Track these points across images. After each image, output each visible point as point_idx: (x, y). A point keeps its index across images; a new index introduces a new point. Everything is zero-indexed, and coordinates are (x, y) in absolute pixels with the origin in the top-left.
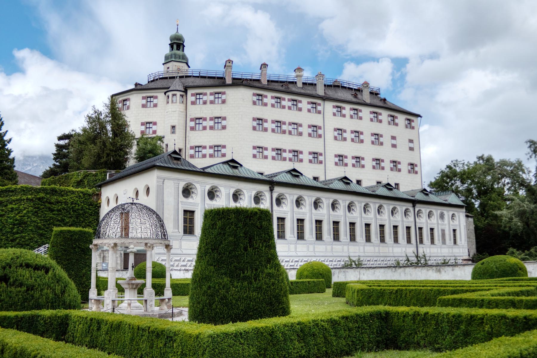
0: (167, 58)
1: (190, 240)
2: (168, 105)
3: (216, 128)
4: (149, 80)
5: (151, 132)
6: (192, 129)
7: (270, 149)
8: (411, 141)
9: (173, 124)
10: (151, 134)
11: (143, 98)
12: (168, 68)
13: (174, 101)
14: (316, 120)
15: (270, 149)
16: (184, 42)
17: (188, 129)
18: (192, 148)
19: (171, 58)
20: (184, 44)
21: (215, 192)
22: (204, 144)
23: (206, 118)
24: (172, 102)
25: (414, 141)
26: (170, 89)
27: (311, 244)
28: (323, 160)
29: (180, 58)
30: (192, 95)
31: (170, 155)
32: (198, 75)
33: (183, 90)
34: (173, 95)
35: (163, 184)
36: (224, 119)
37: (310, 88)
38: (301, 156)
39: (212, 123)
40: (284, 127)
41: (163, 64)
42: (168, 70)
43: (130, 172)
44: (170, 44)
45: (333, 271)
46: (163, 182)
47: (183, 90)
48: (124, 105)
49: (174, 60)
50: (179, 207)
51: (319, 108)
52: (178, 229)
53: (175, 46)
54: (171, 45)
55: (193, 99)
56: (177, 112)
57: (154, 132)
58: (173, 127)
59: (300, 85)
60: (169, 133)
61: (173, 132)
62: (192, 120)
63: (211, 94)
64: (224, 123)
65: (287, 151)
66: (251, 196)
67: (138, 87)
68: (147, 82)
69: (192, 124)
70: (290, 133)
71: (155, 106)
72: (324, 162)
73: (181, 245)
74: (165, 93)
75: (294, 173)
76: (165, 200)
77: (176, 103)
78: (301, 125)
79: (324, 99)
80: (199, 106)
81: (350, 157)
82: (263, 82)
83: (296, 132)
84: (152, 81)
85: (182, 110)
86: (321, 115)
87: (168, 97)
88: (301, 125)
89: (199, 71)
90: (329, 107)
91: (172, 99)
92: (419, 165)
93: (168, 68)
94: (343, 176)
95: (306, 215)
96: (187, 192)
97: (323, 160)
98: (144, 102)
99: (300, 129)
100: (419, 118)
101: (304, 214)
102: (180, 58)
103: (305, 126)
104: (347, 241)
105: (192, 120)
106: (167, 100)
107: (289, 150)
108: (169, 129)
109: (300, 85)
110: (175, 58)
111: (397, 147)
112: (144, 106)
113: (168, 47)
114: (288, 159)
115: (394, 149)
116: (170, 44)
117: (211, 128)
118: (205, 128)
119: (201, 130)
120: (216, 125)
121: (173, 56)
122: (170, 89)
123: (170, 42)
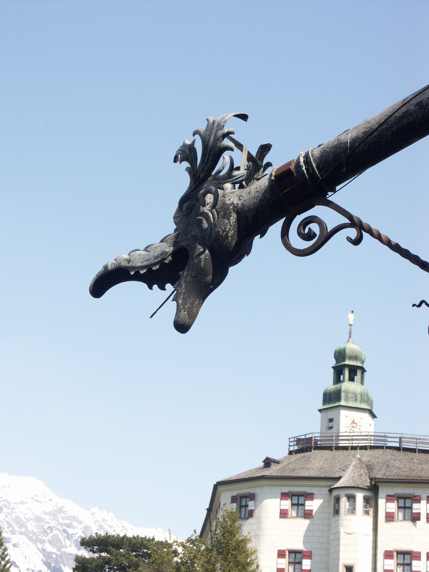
4: (292, 449)
11: (284, 496)
16: (363, 362)
20: (365, 366)
23: (419, 553)
29: (356, 400)
30: (390, 498)
32: (397, 445)
41: (320, 411)
42: (330, 425)
44: (333, 367)
48: (241, 506)
55: (392, 507)
62: (388, 555)
67: (272, 471)
68: (287, 452)
74: (331, 491)
84: (297, 452)
87: (337, 500)
89: (401, 435)
102: (356, 400)
105: (388, 555)
106: (335, 505)
110: (346, 400)
113: (331, 373)
116: (333, 367)
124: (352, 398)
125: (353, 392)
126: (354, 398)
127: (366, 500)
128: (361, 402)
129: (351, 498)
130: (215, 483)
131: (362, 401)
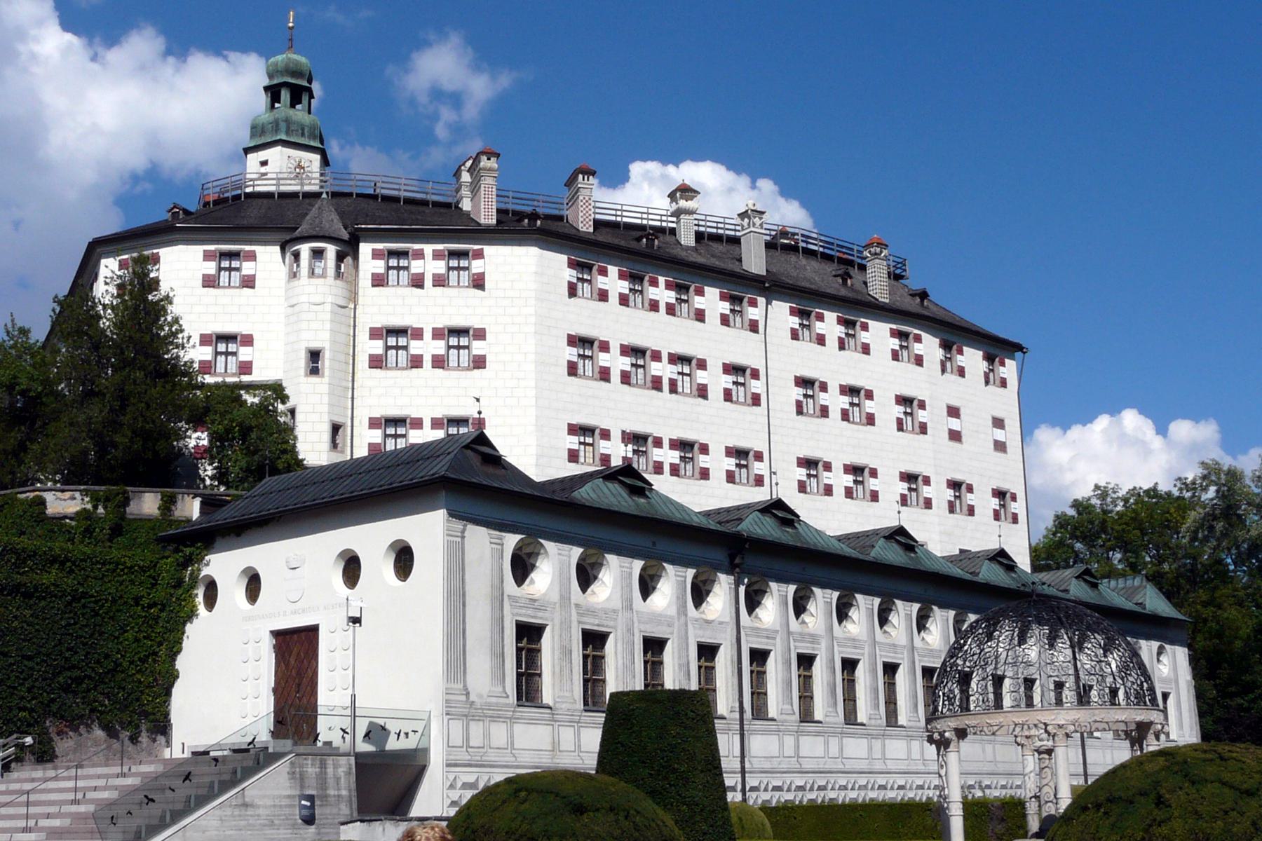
0: (257, 130)
1: (532, 722)
2: (295, 283)
3: (453, 361)
5: (232, 367)
6: (377, 362)
7: (616, 435)
8: (998, 423)
9: (315, 345)
10: (233, 375)
11: (208, 256)
12: (264, 163)
13: (318, 271)
14: (743, 348)
15: (616, 435)
16: (310, 81)
17: (362, 361)
18: (374, 423)
19: (276, 129)
21: (589, 569)
22: (415, 414)
23: (422, 329)
24: (312, 273)
25: (1007, 422)
26: (297, 233)
27: (834, 734)
28: (766, 473)
29: (303, 135)
30: (376, 255)
31: (467, 447)
33: (345, 235)
34: (318, 254)
35: (463, 537)
36: (480, 334)
37: (719, 248)
38: (703, 461)
39: (439, 347)
40: (656, 368)
42: (263, 170)
43: (309, 496)
44: (266, 89)
45: (1044, 814)
46: (463, 532)
47: (345, 235)
49: (284, 137)
50: (505, 612)
51: (753, 313)
52: (504, 687)
53: (285, 95)
54: (273, 92)
55: (379, 266)
56: (328, 307)
57: (246, 368)
58: (315, 355)
59: (687, 238)
60: (302, 372)
61: (314, 371)
62: (375, 334)
63: (437, 255)
64: (478, 347)
65: (666, 443)
66: (685, 581)
69: (377, 347)
70: (673, 388)
71: (249, 282)
72: (767, 481)
73: (512, 737)
75: (780, 514)
76: (467, 588)
77: (323, 276)
78: (702, 365)
79: (771, 287)
80: (400, 290)
81: (838, 467)
82: (581, 225)
83: (687, 385)
85: (342, 303)
86: (760, 336)
87: (297, 256)
88: (702, 365)
90: (780, 315)
91: (310, 265)
92: (1021, 496)
93: (264, 163)
94: (895, 523)
95: (819, 643)
96: (522, 567)
97: (766, 473)
98: (211, 268)
99: (701, 377)
100: (1018, 354)
101: (813, 638)
102: (303, 135)
103: (715, 366)
104: (918, 724)
105: (375, 334)
107: (671, 440)
108: (302, 361)
109: (687, 239)
110: (287, 133)
111: (964, 439)
112: (209, 282)
114: (667, 468)
115: (955, 445)
116: (266, 89)
117: (439, 362)
118: (416, 362)
119: (403, 369)
120: (453, 352)
121: (283, 126)
122: (303, 229)
123: (266, 82)
124: (297, 131)
125: (298, 122)
126: (300, 131)
127: (340, 257)
128: (309, 138)
129: (318, 254)
130: (91, 240)
131: (313, 137)
